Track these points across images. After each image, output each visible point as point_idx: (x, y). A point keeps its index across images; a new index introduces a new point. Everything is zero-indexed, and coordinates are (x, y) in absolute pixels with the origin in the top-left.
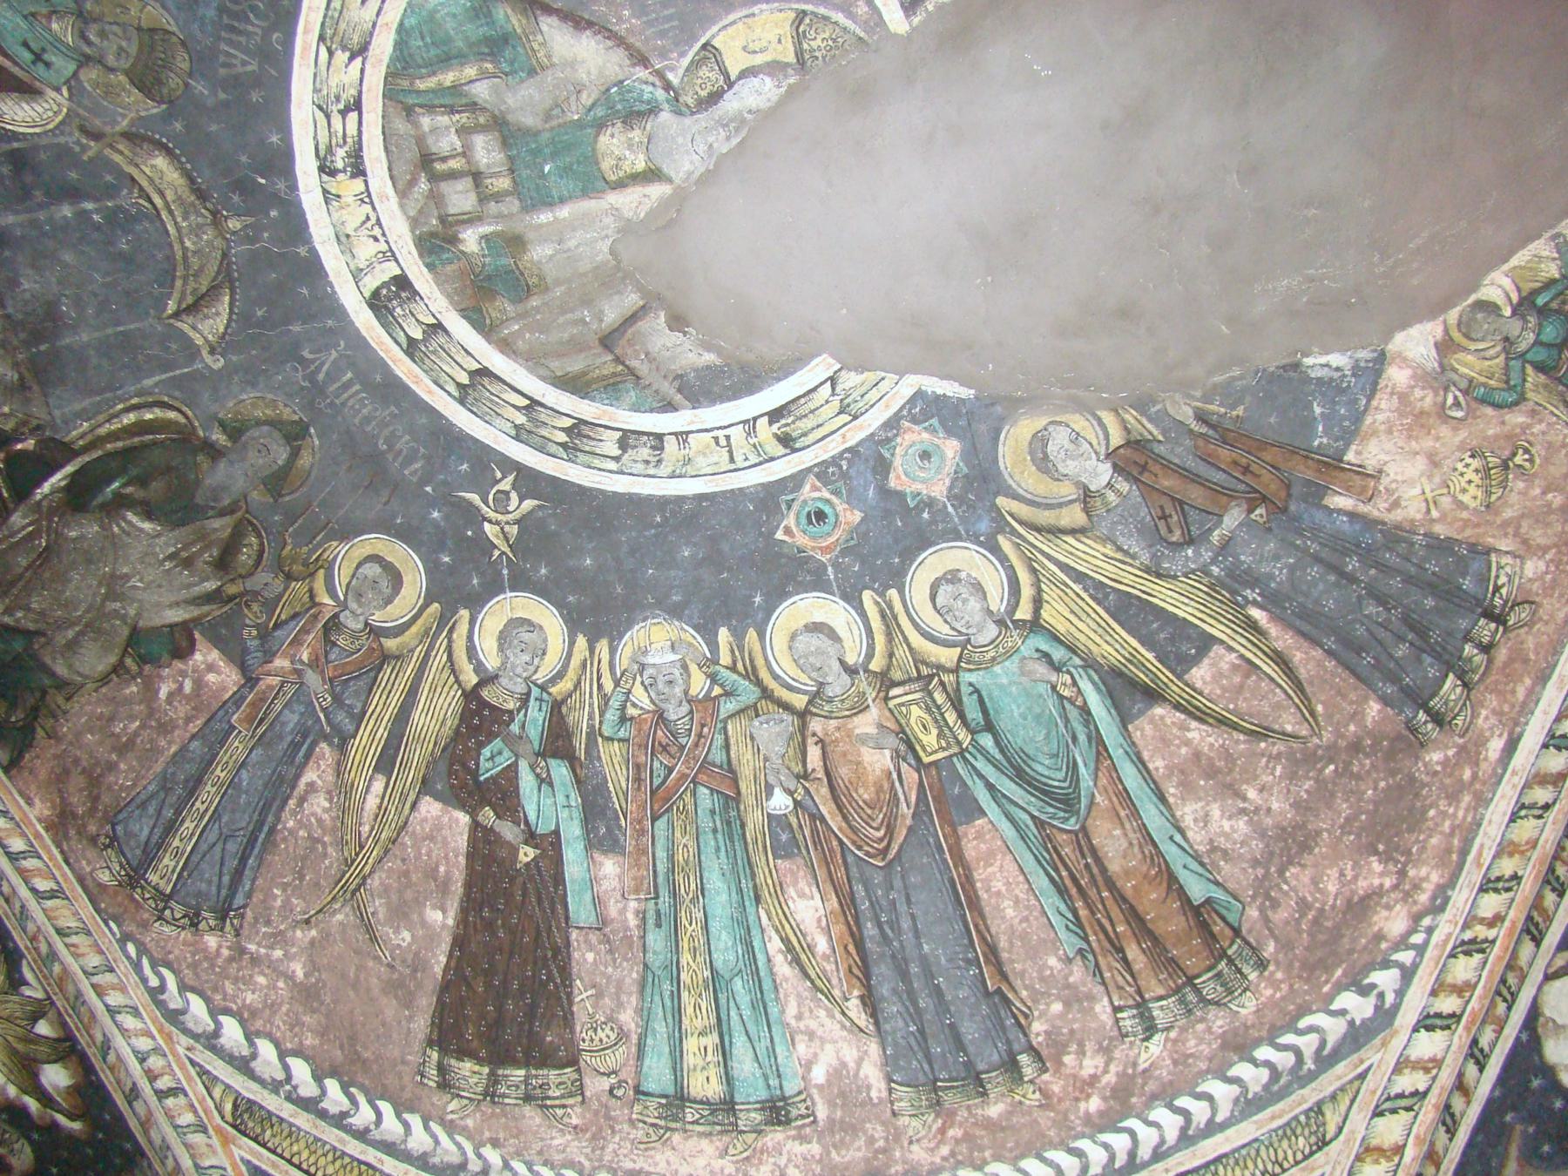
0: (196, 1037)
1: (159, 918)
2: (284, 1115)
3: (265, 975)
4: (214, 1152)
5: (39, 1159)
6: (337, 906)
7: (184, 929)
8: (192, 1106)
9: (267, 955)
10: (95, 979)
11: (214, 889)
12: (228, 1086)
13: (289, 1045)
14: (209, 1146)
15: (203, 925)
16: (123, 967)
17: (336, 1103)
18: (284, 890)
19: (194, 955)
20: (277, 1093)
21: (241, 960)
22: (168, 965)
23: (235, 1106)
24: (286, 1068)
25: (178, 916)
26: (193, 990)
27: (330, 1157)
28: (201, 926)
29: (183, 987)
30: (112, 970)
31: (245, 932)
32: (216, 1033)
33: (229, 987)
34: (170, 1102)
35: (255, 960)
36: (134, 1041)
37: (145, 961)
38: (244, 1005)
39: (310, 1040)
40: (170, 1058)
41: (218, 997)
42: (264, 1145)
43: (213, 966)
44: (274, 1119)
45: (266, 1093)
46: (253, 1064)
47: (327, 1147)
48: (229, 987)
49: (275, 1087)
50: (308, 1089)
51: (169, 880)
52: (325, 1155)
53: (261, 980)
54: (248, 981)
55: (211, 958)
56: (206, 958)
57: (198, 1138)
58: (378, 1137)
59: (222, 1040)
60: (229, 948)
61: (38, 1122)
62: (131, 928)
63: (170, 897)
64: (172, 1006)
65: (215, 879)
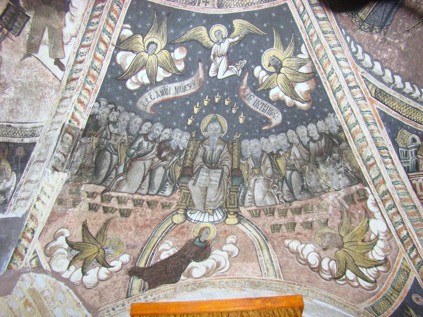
0: (365, 68)
1: (360, 28)
2: (391, 94)
3: (391, 48)
4: (368, 106)
5: (284, 119)
6: (419, 26)
7: (367, 32)
8: (361, 91)
9: (393, 42)
10: (333, 49)
11: (380, 19)
12: (374, 85)
13: (396, 71)
14: (366, 104)
15: (374, 31)
16: (344, 45)
17: (408, 90)
18: (403, 20)
19: (369, 41)
20: (390, 87)
21: (384, 43)
22: (360, 44)
23: (376, 91)
24: (394, 79)
25: (366, 28)
26: (367, 53)
27: (405, 107)
28: (373, 32)
29: (364, 52)
30: (340, 46)
31: (388, 34)
32: (372, 68)
33: (379, 52)
34: (353, 90)
35: (389, 43)
36: (343, 70)
37: (352, 43)
38: (383, 58)
39: (402, 70)
40: (355, 76)
41: (375, 55)
42: (384, 104)
43: (375, 45)
44: (388, 95)
45: (386, 87)
46: (383, 78)
47: (404, 104)
48: (379, 52)
49: (389, 85)
50: (399, 85)
51: (366, 15)
52: (403, 106)
53: (390, 50)
54: (386, 50)
55: (375, 42)
56: (373, 42)
57: (362, 102)
58: (420, 100)
59: (374, 70)
60: (381, 39)
61: (288, 105)
62: (350, 31)
63: (365, 21)
64: (359, 58)
65: (382, 16)
